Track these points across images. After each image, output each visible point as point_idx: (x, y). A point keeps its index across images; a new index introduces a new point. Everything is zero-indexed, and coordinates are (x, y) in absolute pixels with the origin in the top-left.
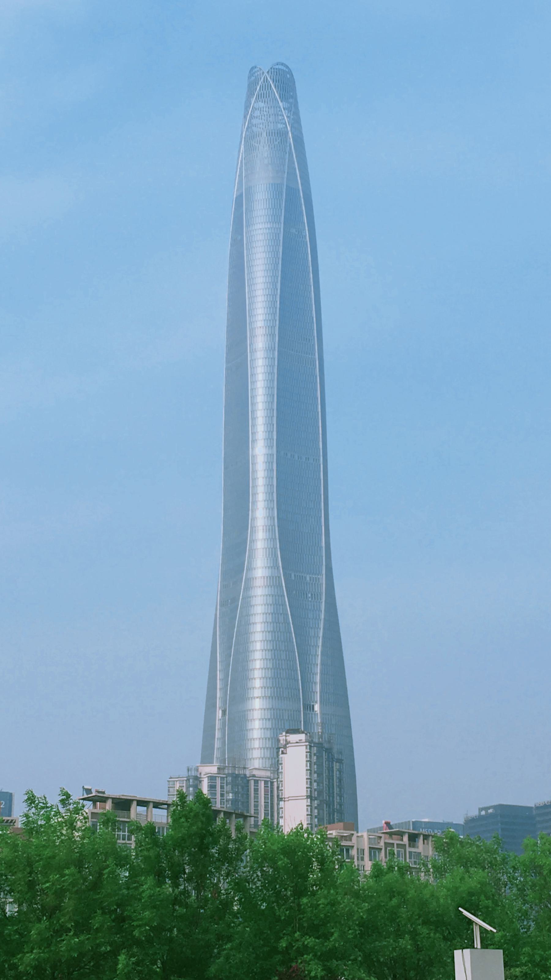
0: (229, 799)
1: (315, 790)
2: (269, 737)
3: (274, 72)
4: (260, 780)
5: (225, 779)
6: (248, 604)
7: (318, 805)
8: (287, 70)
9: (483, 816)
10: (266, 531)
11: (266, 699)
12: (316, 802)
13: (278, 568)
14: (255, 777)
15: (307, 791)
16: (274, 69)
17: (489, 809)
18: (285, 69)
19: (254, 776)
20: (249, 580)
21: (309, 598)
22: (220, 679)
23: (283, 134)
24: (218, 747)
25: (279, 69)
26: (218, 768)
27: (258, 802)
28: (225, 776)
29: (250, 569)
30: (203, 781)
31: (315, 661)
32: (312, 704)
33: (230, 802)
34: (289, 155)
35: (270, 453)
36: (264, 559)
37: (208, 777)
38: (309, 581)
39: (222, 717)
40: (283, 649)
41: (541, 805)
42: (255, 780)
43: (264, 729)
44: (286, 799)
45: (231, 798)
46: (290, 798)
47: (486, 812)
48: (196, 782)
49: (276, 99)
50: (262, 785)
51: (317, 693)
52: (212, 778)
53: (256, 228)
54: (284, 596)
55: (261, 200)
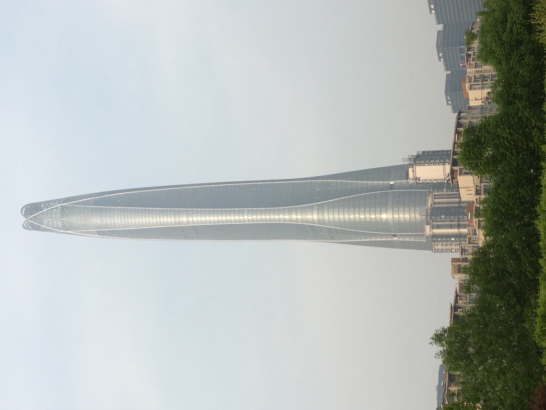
0: (444, 217)
1: (440, 161)
2: (408, 208)
3: (26, 214)
4: (434, 201)
5: (433, 220)
6: (334, 223)
7: (448, 159)
8: (25, 207)
9: (451, 103)
10: (292, 213)
11: (387, 210)
12: (446, 161)
13: (312, 206)
14: (432, 204)
15: (440, 165)
16: (24, 214)
17: (448, 99)
18: (25, 208)
19: (431, 205)
20: (319, 222)
21: (329, 188)
22: (376, 239)
23: (63, 208)
24: (414, 239)
25: (25, 211)
26: (427, 225)
27: (446, 202)
28: (431, 220)
29: (313, 221)
30: (434, 232)
31: (365, 184)
32: (390, 185)
33: (446, 217)
34: (75, 205)
35: (247, 211)
36: (308, 214)
37: (432, 229)
38: (320, 189)
39: (397, 237)
40: (359, 202)
41: (445, 67)
42: (434, 204)
43: (404, 211)
44: (445, 177)
45: (444, 217)
46: (445, 175)
47: (450, 101)
48: (435, 237)
49: (42, 213)
50: (436, 200)
51: (383, 183)
52: (433, 227)
53: (117, 222)
54: (329, 202)
55: (101, 220)
